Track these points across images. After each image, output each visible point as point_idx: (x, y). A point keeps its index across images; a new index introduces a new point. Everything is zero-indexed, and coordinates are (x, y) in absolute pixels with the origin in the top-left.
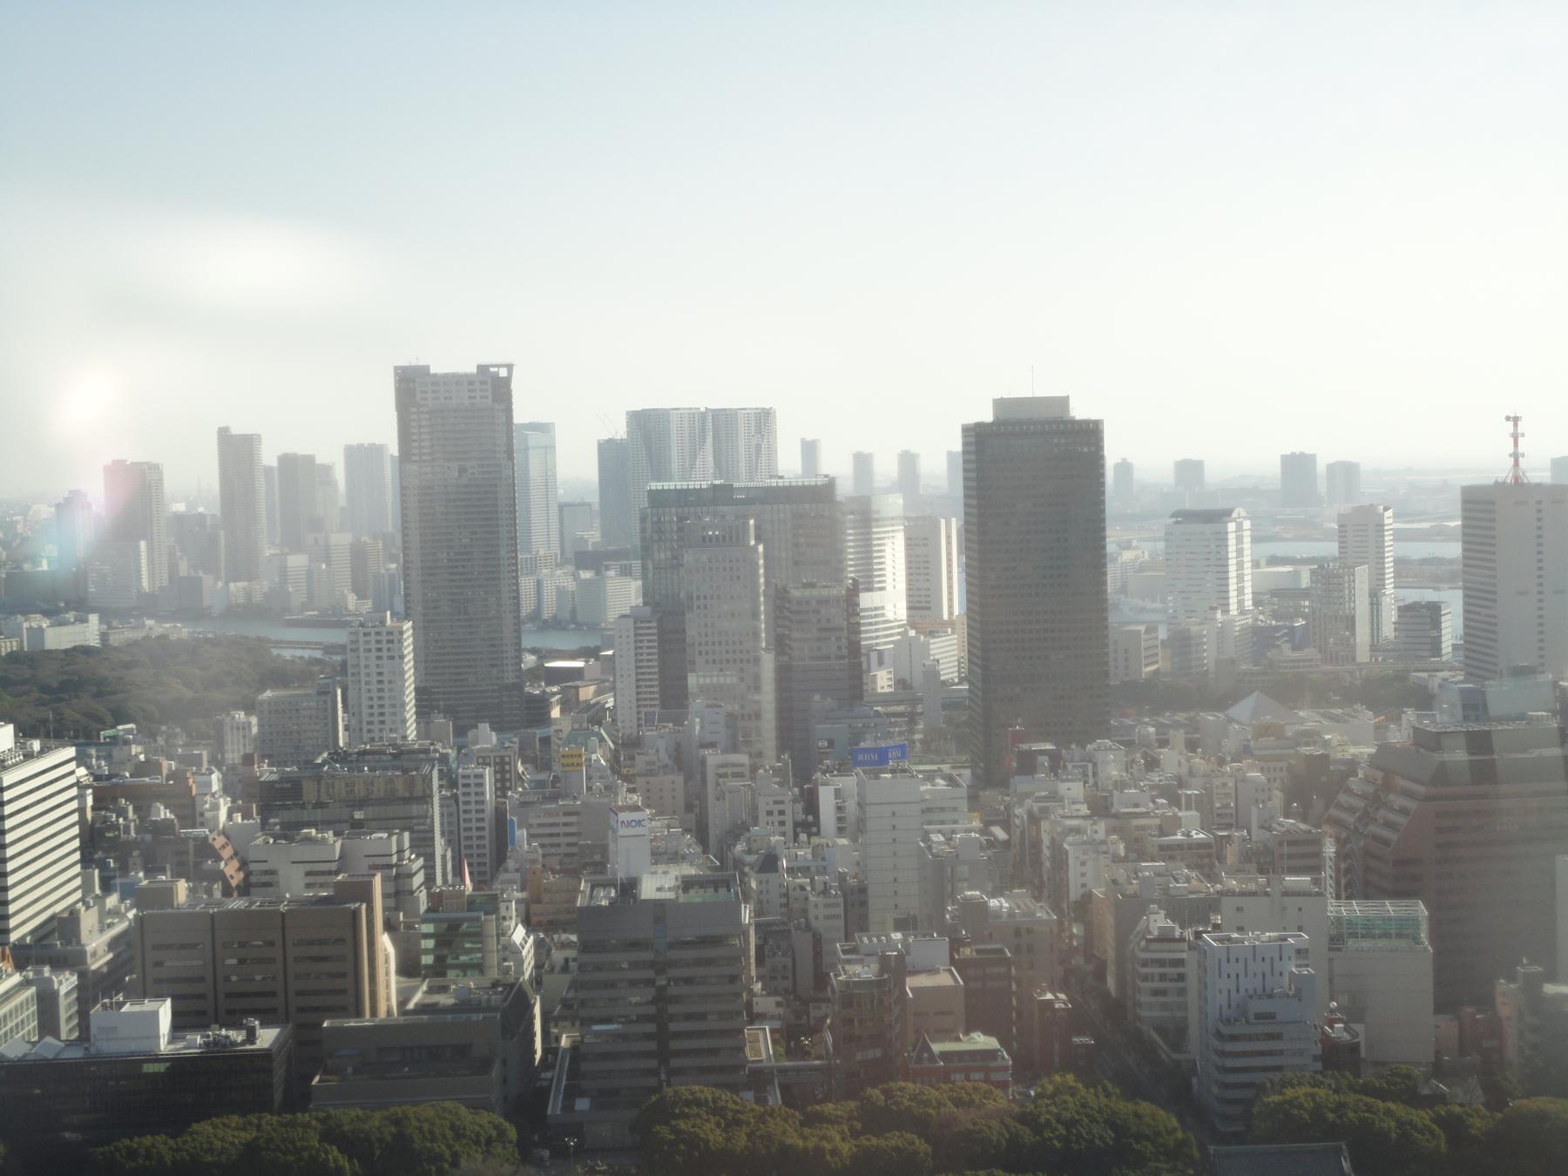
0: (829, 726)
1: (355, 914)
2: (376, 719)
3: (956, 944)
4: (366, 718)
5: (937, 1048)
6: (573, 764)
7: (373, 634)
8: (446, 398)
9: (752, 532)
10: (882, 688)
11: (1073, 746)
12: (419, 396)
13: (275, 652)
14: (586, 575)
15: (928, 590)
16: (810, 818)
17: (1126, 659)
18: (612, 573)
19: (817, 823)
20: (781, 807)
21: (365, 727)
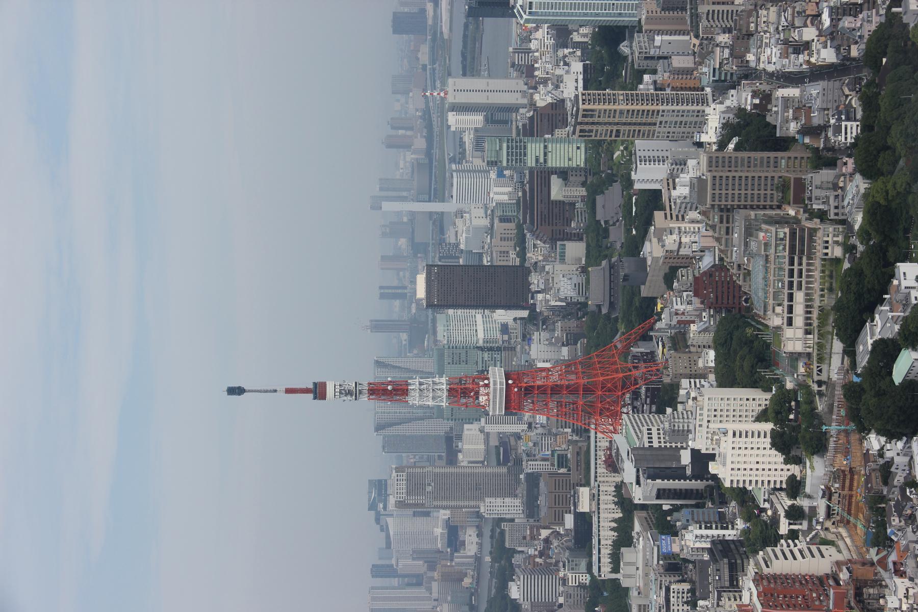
2: (515, 508)
3: (563, 345)
12: (401, 500)
14: (460, 456)
17: (508, 230)
21: (518, 512)
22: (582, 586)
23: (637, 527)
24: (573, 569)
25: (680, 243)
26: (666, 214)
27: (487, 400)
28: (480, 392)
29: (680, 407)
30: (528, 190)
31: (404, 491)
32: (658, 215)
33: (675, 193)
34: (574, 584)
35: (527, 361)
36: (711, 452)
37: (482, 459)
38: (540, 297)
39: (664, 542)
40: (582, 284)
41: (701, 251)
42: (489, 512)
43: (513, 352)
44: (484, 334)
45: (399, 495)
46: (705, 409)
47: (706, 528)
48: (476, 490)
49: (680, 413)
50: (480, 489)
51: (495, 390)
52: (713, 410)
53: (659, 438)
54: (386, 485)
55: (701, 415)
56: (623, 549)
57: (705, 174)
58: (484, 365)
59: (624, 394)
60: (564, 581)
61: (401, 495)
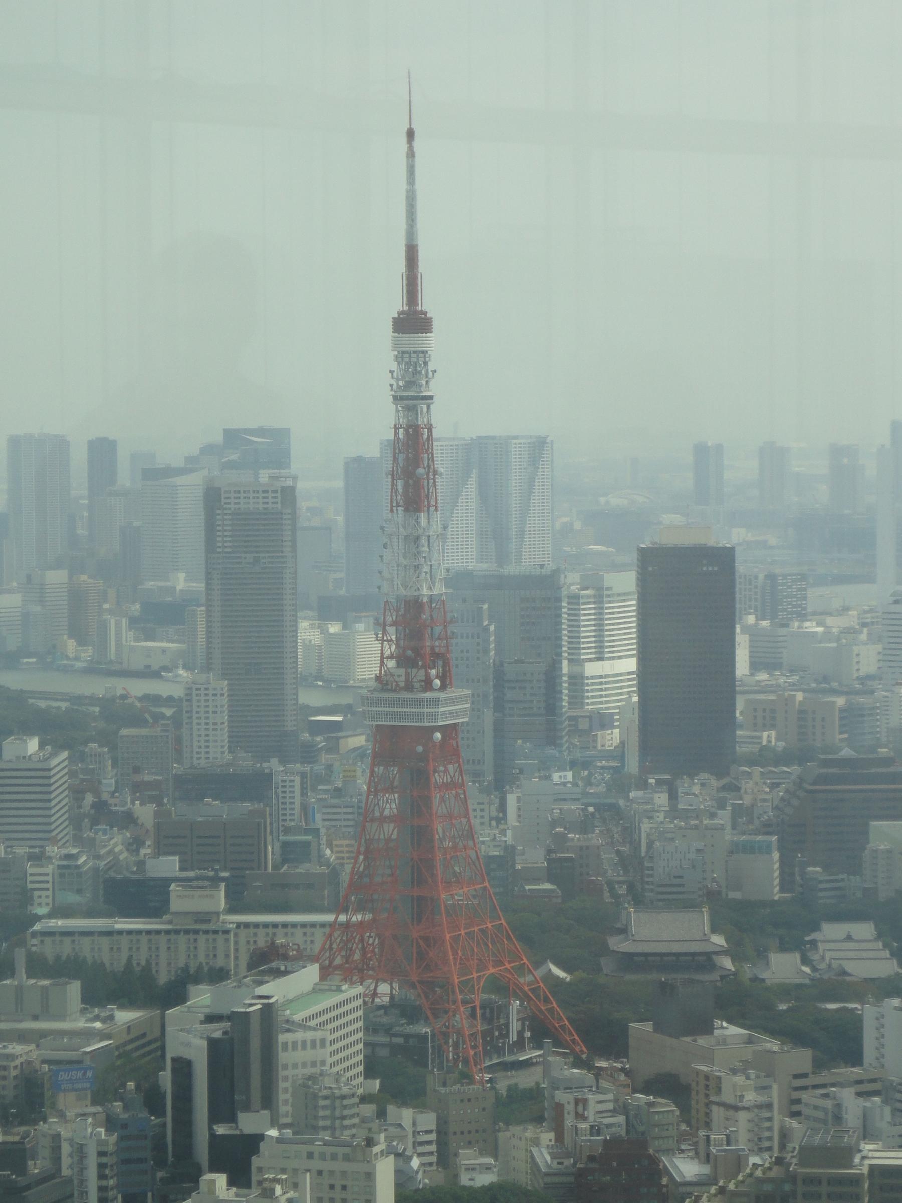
1: (259, 824)
2: (204, 750)
3: (549, 851)
4: (196, 749)
5: (527, 887)
7: (203, 689)
9: (485, 615)
10: (603, 746)
12: (223, 501)
13: (31, 701)
14: (334, 628)
16: (501, 815)
17: (823, 727)
18: (361, 626)
19: (505, 817)
20: (482, 806)
21: (195, 756)
22: (26, 897)
23: (124, 1016)
24: (62, 876)
25: (736, 1108)
26: (805, 1075)
27: (398, 685)
28: (415, 671)
29: (369, 1110)
30: (892, 770)
32: (802, 1058)
33: (847, 1096)
34: (29, 878)
36: (255, 1178)
38: (662, 799)
39: (80, 1074)
40: (683, 893)
41: (708, 1155)
42: (194, 692)
44: (593, 677)
45: (232, 495)
46: (348, 1167)
47: (101, 1166)
49: (355, 1110)
51: (420, 703)
52: (344, 1183)
53: (304, 1065)
55: (334, 1157)
56: (74, 989)
57: (867, 1162)
59: (413, 986)
60: (38, 858)
61: (232, 501)
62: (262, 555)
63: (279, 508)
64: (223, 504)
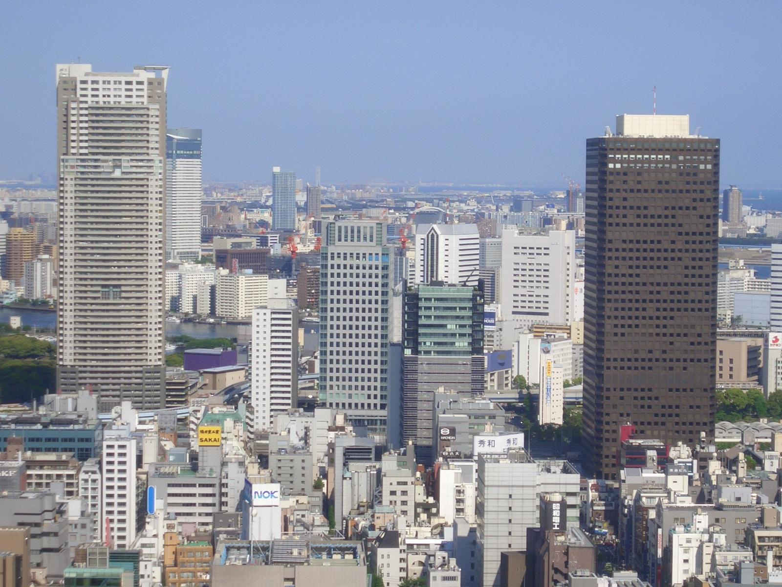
0: (452, 416)
6: (210, 440)
8: (104, 96)
11: (680, 443)
12: (79, 92)
14: (224, 272)
15: (547, 296)
16: (431, 500)
17: (731, 369)
19: (436, 505)
20: (403, 488)
31: (101, 99)
35: (453, 432)
37: (218, 311)
43: (468, 387)
48: (103, 286)
50: (106, 296)
54: (192, 156)
58: (433, 304)
61: (89, 92)
62: (123, 157)
63: (145, 103)
64: (78, 96)
